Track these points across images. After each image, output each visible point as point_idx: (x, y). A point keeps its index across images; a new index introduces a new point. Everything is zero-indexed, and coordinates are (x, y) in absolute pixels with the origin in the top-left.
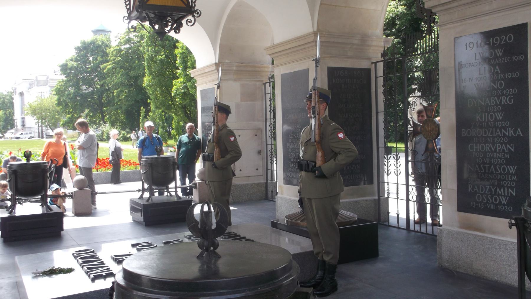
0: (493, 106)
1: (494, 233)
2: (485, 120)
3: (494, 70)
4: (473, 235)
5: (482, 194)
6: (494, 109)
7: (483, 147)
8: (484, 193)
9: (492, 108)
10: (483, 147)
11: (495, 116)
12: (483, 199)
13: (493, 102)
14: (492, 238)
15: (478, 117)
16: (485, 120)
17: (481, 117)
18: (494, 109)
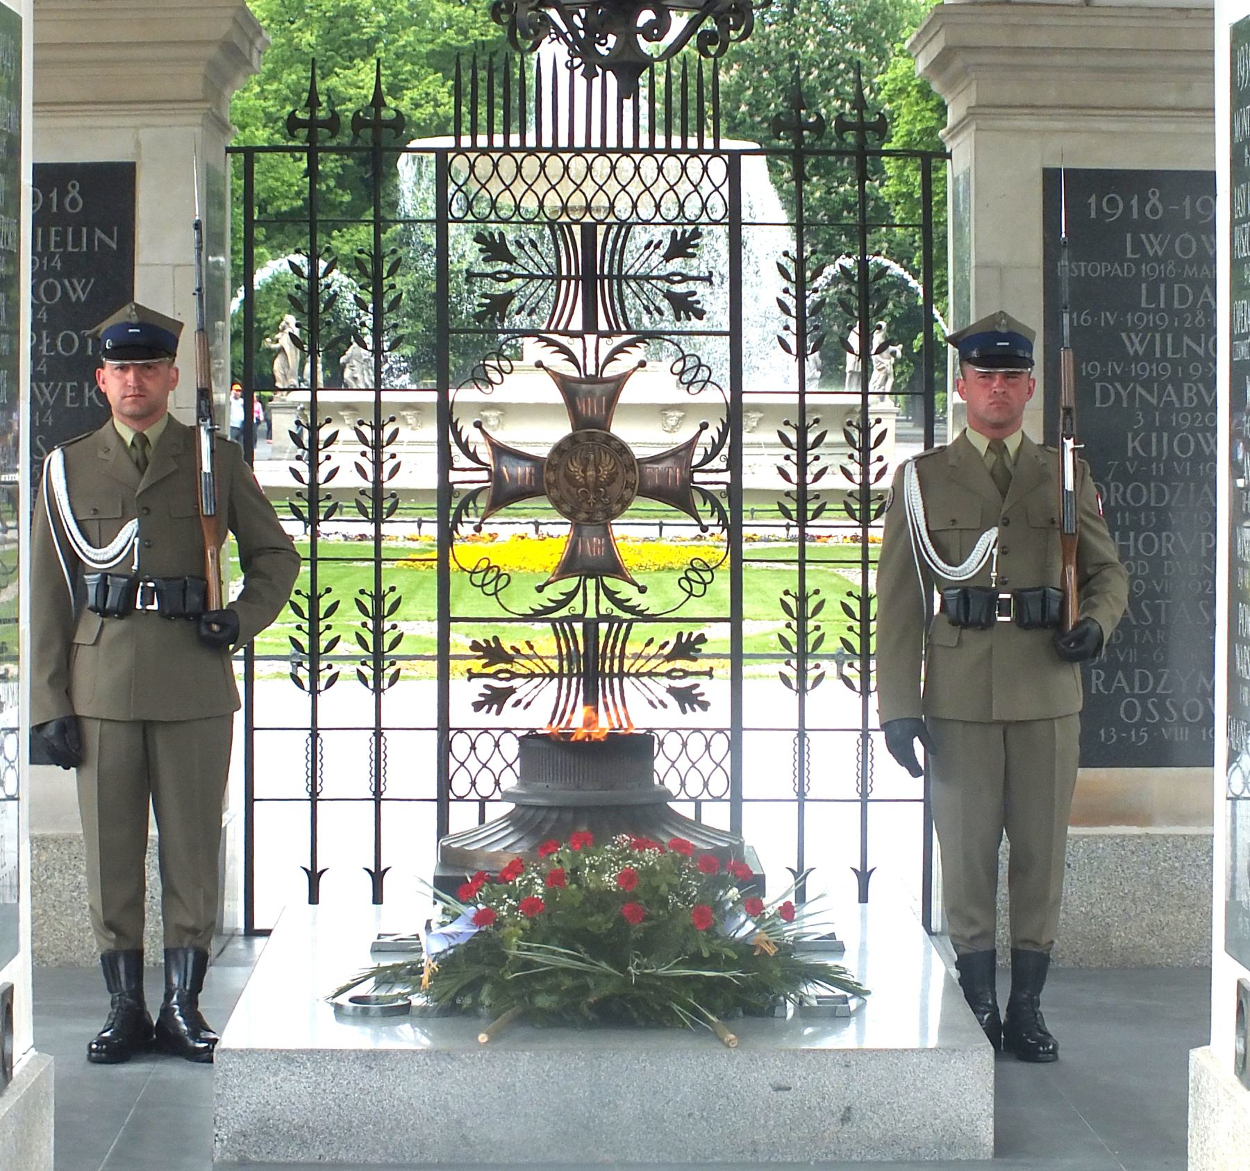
0: (1192, 411)
1: (1182, 819)
2: (1160, 453)
3: (1196, 299)
4: (1112, 837)
5: (1143, 699)
6: (1194, 420)
7: (1149, 544)
8: (1153, 693)
9: (1185, 418)
10: (1149, 544)
11: (1198, 443)
12: (1146, 711)
13: (1191, 400)
14: (1184, 836)
15: (1132, 444)
16: (1160, 453)
17: (1146, 445)
18: (1194, 420)
